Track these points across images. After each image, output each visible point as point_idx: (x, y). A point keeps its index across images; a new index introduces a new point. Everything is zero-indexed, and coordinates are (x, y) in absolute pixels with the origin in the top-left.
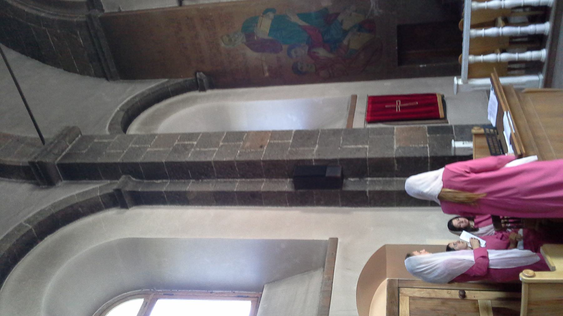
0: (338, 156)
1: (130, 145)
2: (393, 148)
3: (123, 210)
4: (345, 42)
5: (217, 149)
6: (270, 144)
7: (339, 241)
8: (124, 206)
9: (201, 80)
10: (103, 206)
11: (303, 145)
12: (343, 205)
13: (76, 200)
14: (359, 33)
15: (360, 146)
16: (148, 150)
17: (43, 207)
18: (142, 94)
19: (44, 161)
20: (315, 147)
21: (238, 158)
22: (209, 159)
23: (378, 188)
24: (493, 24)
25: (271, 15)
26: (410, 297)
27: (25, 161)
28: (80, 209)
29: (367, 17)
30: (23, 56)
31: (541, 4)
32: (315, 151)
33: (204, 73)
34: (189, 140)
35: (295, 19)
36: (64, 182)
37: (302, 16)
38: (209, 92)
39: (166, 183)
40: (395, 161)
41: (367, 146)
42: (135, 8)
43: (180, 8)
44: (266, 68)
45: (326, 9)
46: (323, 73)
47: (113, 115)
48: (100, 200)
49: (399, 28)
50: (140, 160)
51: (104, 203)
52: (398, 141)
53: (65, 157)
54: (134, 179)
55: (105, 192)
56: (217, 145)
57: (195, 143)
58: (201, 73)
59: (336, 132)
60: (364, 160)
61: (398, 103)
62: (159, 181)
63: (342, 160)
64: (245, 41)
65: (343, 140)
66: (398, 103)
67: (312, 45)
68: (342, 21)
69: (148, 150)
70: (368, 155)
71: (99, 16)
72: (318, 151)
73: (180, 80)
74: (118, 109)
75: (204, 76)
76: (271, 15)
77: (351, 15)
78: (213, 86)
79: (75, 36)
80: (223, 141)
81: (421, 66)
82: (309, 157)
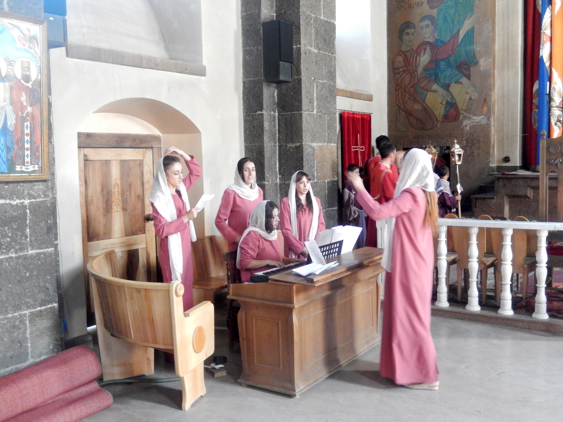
2: (313, 141)
4: (435, 87)
7: (202, 78)
11: (317, 33)
12: (244, 83)
15: (315, 104)
20: (315, 49)
23: (266, 125)
24: (451, 250)
26: (142, 160)
29: (462, 112)
31: (469, 298)
32: (310, 48)
37: (470, 34)
40: (298, 144)
41: (315, 112)
45: (477, 63)
46: (400, 59)
52: (321, 148)
59: (332, 75)
60: (299, 108)
61: (362, 149)
63: (300, 81)
65: (322, 84)
66: (362, 149)
67: (433, 46)
68: (461, 83)
70: (305, 114)
72: (310, 52)
77: (467, 93)
82: (302, 41)
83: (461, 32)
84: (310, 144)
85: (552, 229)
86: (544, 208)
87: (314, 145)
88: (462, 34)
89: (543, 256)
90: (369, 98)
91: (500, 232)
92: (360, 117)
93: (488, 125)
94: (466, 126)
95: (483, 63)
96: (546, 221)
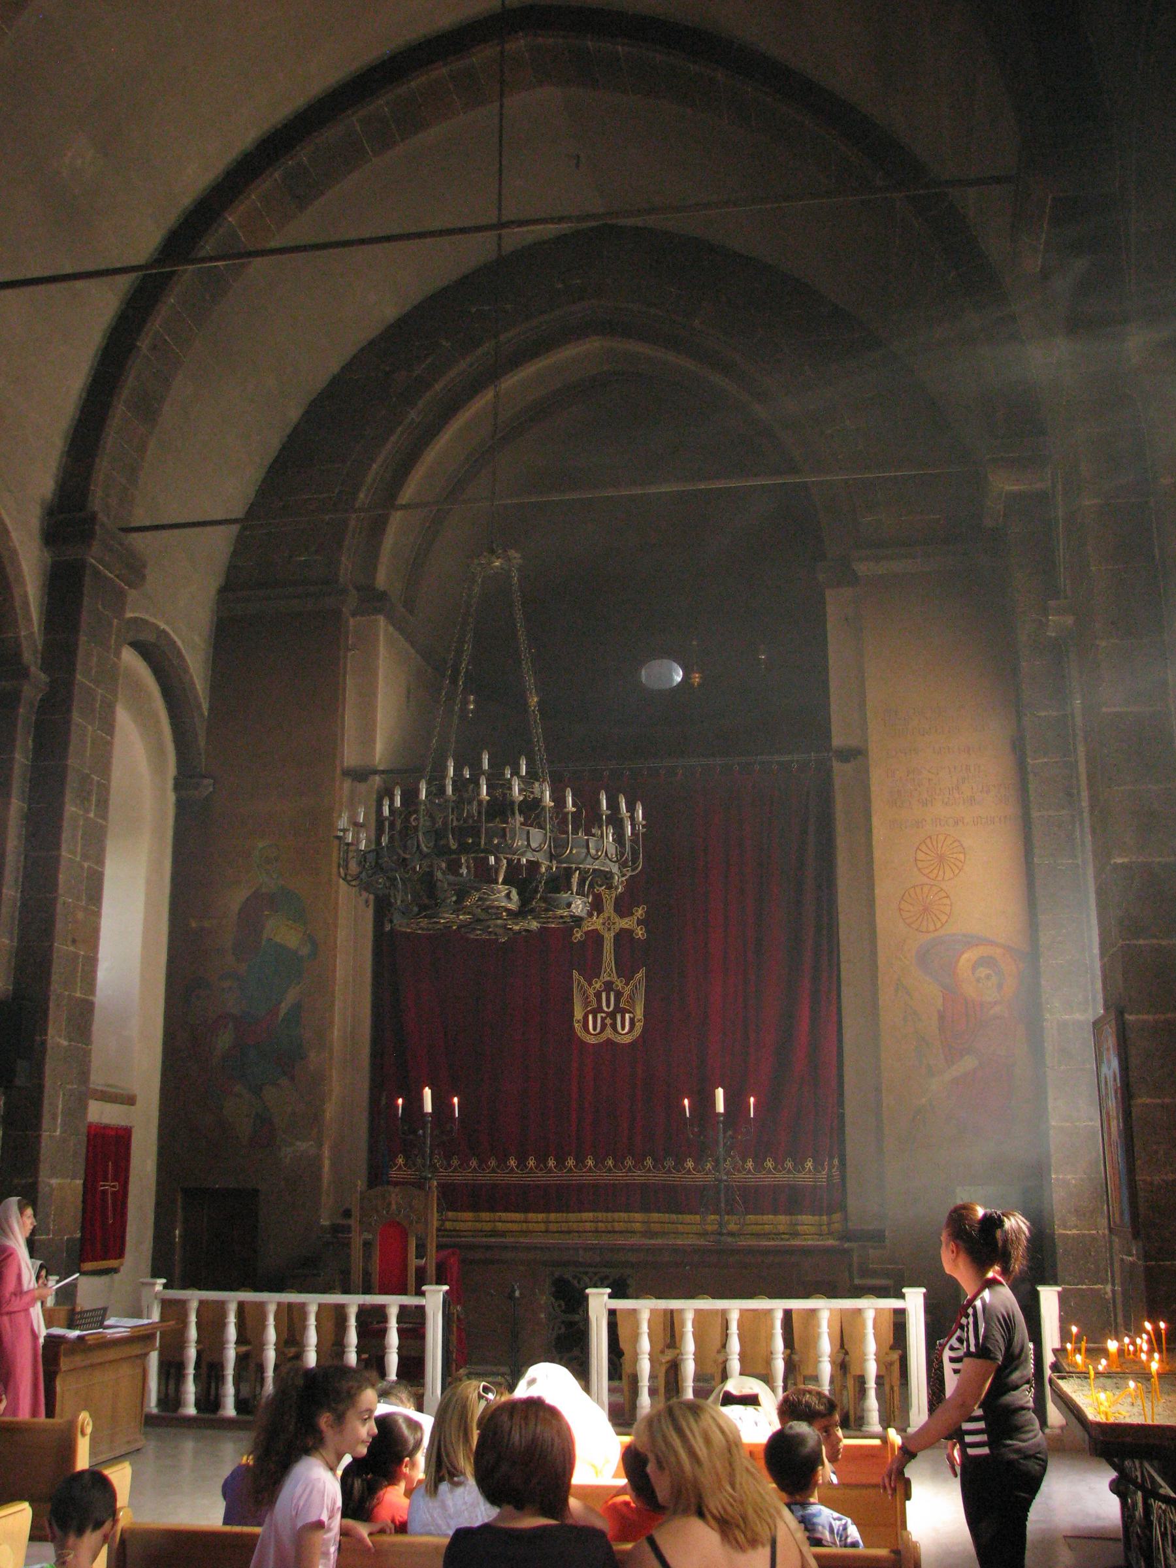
0: (48, 1082)
2: (53, 1175)
4: (238, 1088)
5: (78, 859)
6: (76, 956)
13: (17, 592)
14: (252, 1116)
16: (90, 728)
17: (14, 535)
18: (186, 670)
21: (61, 900)
22: (64, 846)
25: (305, 951)
27: (97, 500)
30: (288, 430)
32: (58, 1040)
34: (98, 801)
35: (291, 997)
36: (49, 561)
38: (171, 797)
39: (27, 758)
41: (58, 1133)
42: (349, 682)
43: (339, 771)
44: (207, 924)
47: (152, 620)
48: (11, 635)
49: (255, 1192)
50: (76, 717)
54: (39, 698)
55: (25, 643)
56: (85, 857)
57: (92, 815)
59: (84, 1076)
61: (114, 1186)
64: (264, 890)
66: (114, 1186)
69: (90, 728)
70: (45, 1135)
72: (58, 1044)
73: (202, 742)
74: (163, 626)
76: (305, 951)
78: (181, 806)
79: (313, 549)
80: (90, 868)
81: (177, 1232)
82: (51, 1031)
83: (283, 1005)
84: (48, 1180)
85: (361, 1302)
86: (357, 1277)
87: (54, 1181)
88: (284, 1008)
89: (352, 1338)
90: (130, 1100)
91: (302, 1307)
92: (113, 1133)
93: (319, 1157)
94: (286, 1157)
95: (312, 1055)
96: (358, 1294)
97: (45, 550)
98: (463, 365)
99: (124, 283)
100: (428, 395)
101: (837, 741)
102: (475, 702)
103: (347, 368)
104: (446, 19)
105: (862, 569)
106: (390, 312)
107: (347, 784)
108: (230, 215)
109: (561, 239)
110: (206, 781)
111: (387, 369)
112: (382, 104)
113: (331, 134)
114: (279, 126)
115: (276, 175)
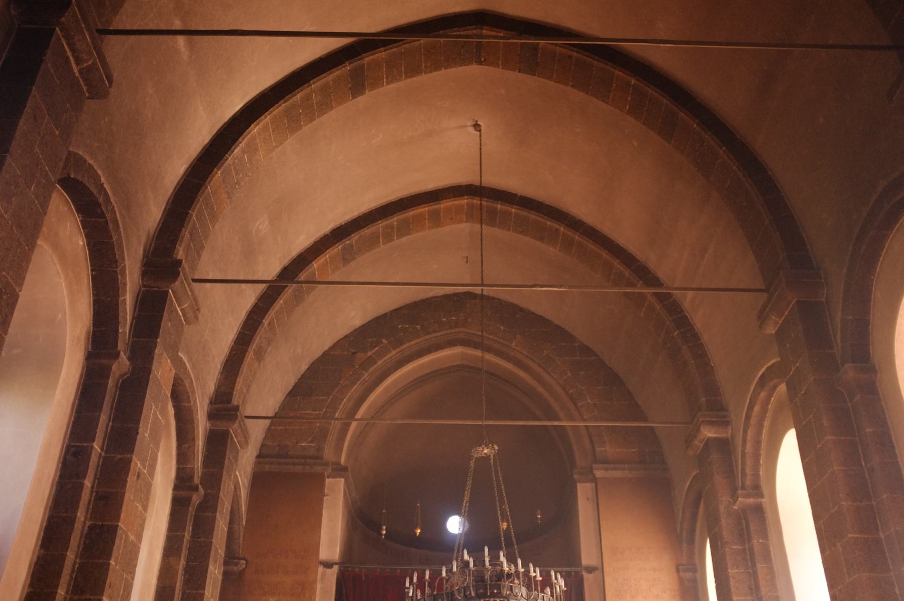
1: (226, 503)
3: (172, 484)
8: (176, 488)
9: (237, 564)
10: (181, 466)
18: (241, 497)
19: (237, 422)
28: (187, 445)
33: (244, 569)
42: (324, 512)
48: (189, 466)
51: (183, 468)
53: (232, 436)
57: (216, 572)
58: (244, 566)
62: (191, 528)
71: (325, 474)
75: (241, 569)
79: (310, 439)
97: (207, 422)
98: (394, 352)
99: (261, 287)
100: (375, 367)
101: (585, 562)
102: (386, 530)
103: (332, 348)
104: (431, 185)
105: (599, 474)
106: (358, 323)
107: (321, 569)
108: (315, 263)
109: (447, 297)
110: (243, 562)
111: (353, 351)
112: (394, 220)
113: (367, 231)
114: (343, 224)
115: (340, 247)
